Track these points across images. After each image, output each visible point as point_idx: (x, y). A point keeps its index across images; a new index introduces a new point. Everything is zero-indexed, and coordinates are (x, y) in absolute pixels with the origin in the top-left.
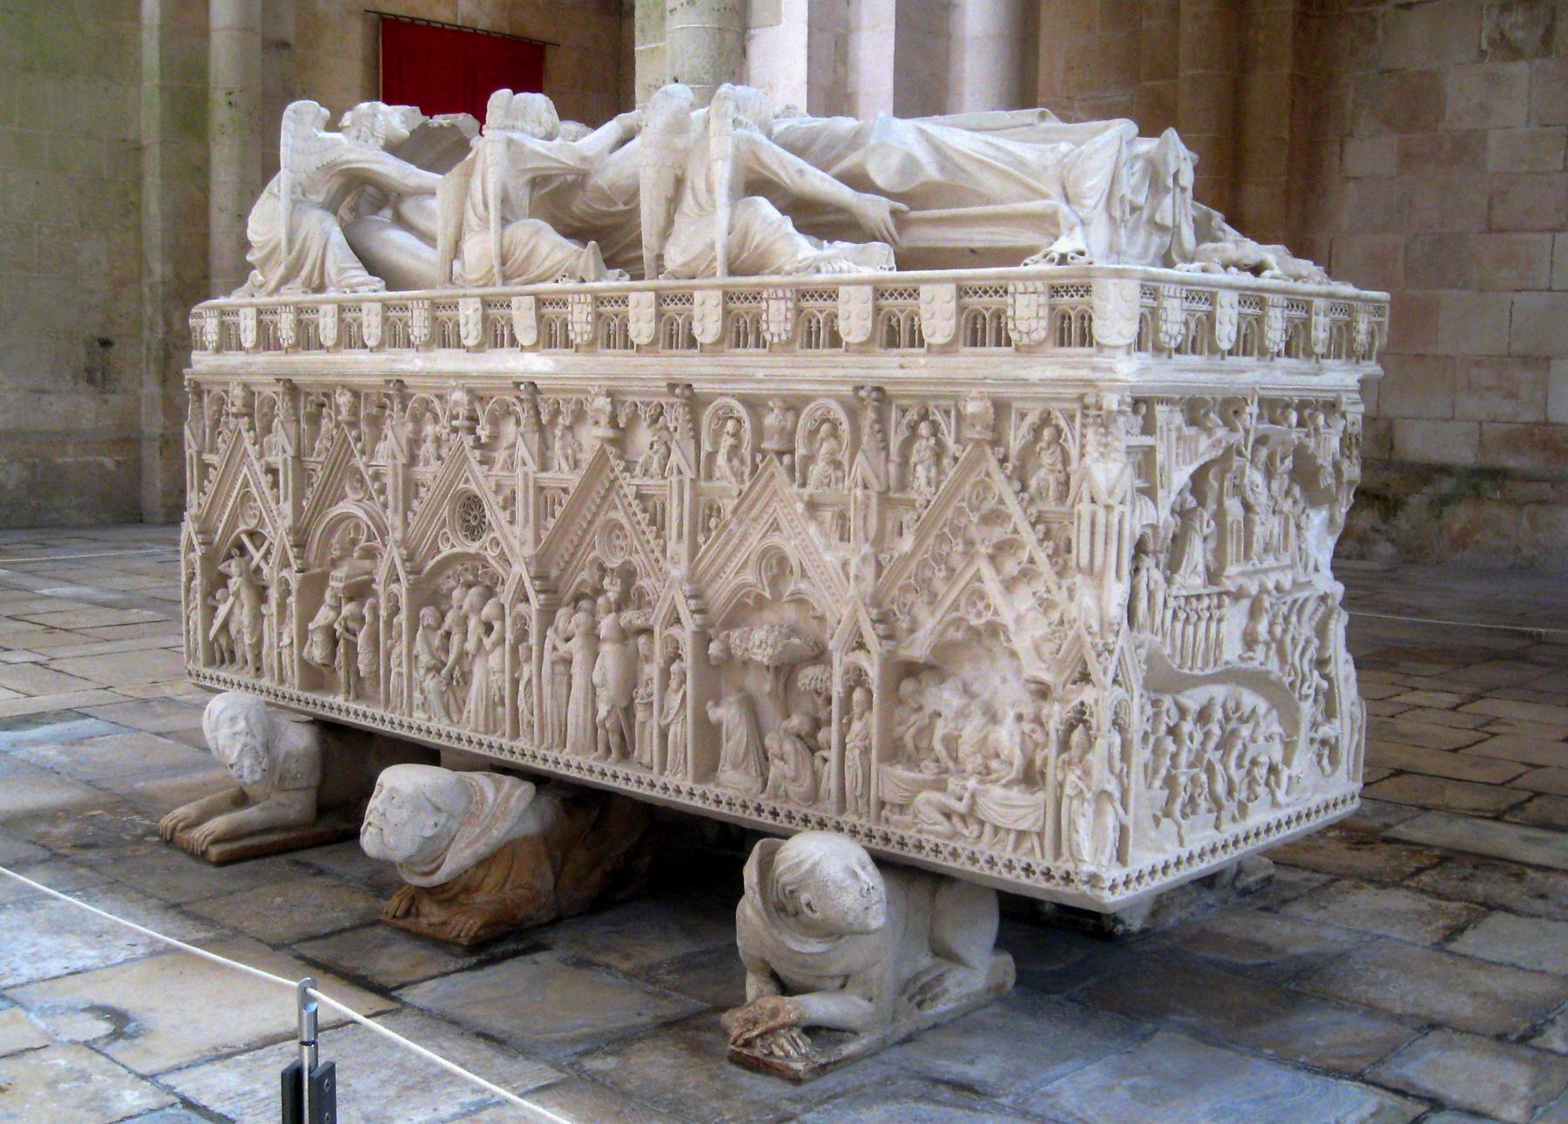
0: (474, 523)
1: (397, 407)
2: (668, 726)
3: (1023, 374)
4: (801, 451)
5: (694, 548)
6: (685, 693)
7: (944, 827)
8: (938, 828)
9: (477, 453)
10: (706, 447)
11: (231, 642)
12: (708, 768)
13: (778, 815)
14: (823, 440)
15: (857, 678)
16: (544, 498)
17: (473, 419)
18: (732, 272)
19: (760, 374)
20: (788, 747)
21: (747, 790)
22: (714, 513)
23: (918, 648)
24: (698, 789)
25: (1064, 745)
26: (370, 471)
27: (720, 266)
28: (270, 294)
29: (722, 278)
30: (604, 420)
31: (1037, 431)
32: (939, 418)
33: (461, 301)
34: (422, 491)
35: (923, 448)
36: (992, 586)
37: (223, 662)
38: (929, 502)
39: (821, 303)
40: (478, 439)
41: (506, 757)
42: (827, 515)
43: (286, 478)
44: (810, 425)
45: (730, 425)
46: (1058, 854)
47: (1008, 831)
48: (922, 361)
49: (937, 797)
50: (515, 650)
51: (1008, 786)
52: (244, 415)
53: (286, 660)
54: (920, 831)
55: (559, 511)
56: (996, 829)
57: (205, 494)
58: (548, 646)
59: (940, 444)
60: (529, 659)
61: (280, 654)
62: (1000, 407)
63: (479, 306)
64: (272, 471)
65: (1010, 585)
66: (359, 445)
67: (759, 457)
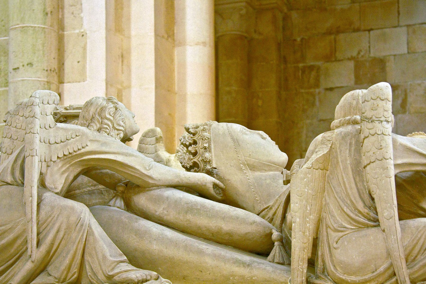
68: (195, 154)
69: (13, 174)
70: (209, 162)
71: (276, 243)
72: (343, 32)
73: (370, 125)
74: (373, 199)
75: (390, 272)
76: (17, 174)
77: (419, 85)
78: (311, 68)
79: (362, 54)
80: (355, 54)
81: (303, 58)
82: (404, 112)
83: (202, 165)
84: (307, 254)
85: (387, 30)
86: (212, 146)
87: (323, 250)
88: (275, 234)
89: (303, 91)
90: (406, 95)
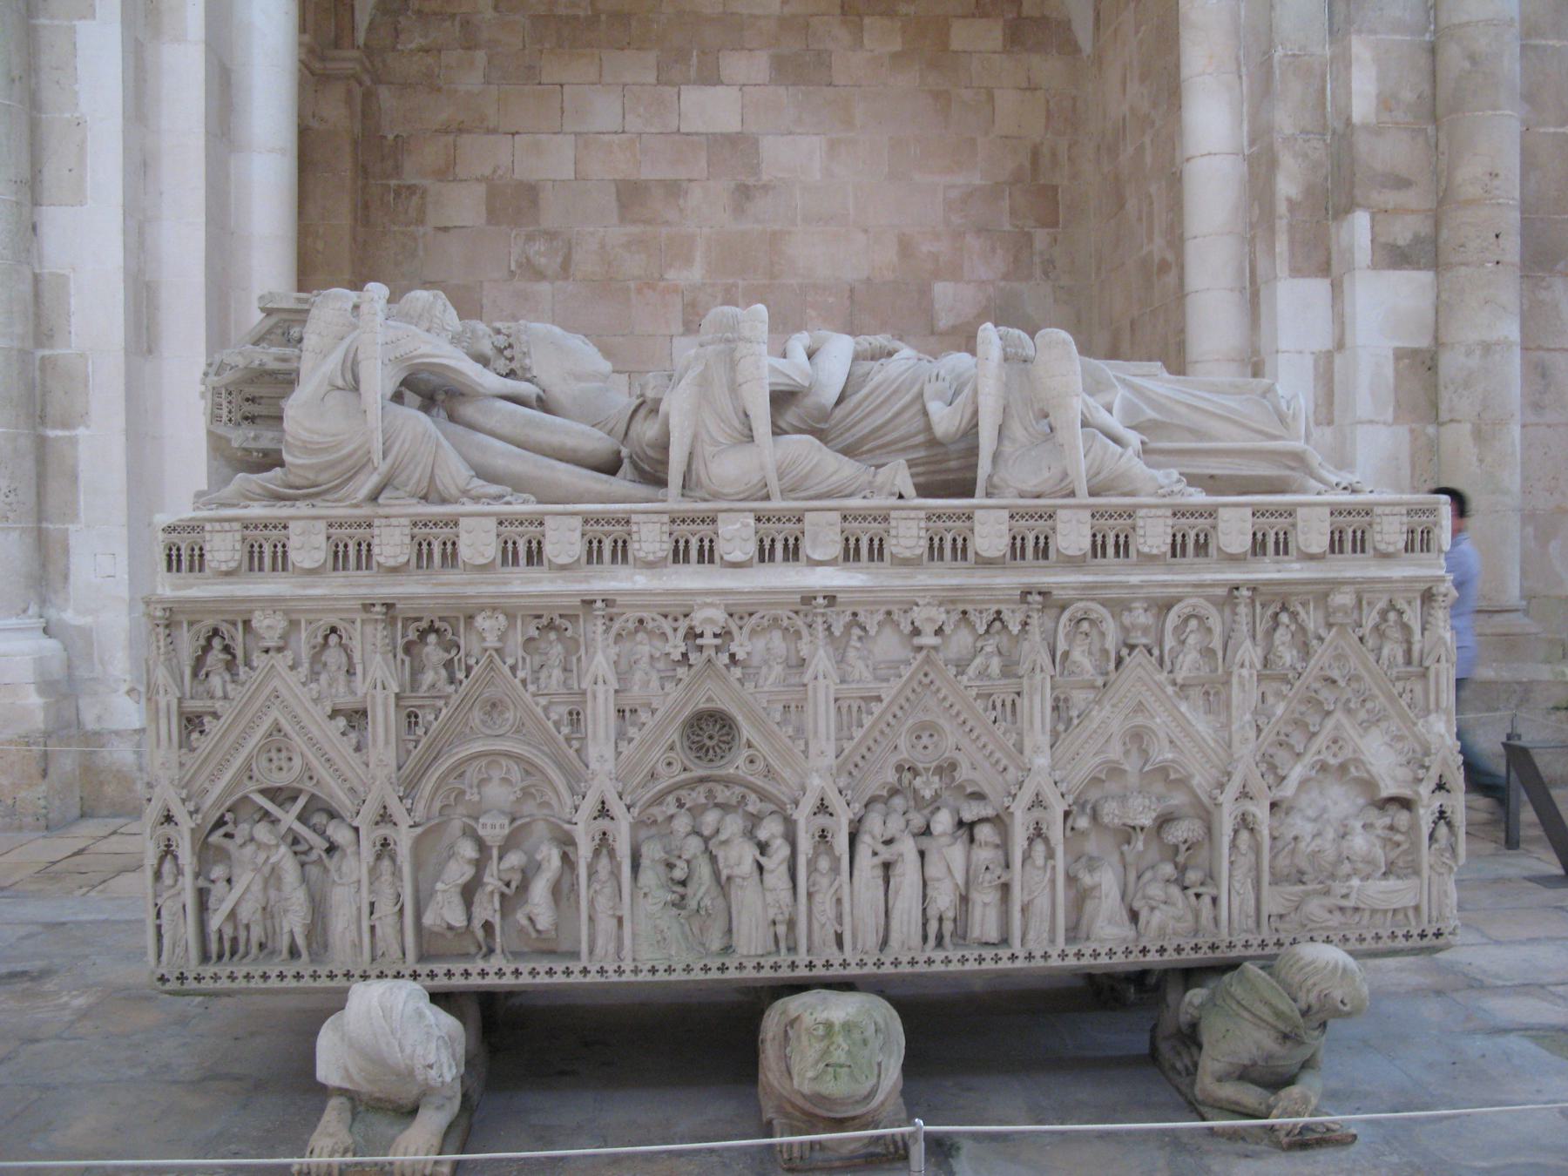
0: (709, 743)
1: (600, 629)
2: (1030, 902)
3: (1385, 574)
4: (1169, 642)
5: (1055, 735)
6: (1054, 868)
7: (1336, 919)
8: (1330, 923)
9: (737, 672)
10: (1062, 646)
11: (236, 928)
12: (1073, 933)
13: (1165, 950)
14: (1192, 631)
15: (1245, 823)
16: (850, 710)
17: (725, 634)
18: (1091, 494)
19: (1134, 579)
20: (1175, 891)
21: (1125, 940)
22: (1061, 704)
23: (1288, 790)
24: (1071, 950)
25: (1432, 837)
26: (543, 701)
27: (1082, 488)
28: (356, 506)
29: (1083, 498)
30: (929, 629)
31: (1383, 615)
32: (1300, 609)
33: (721, 516)
34: (644, 716)
35: (1281, 636)
36: (1350, 731)
37: (220, 957)
38: (1300, 674)
39: (1192, 520)
40: (732, 656)
41: (802, 972)
42: (1195, 693)
43: (384, 720)
44: (1177, 621)
45: (1085, 626)
46: (1429, 922)
47: (1385, 911)
48: (1297, 566)
49: (1329, 901)
50: (812, 865)
51: (1379, 879)
52: (280, 650)
53: (386, 929)
54: (1310, 930)
55: (868, 721)
56: (1374, 912)
57: (193, 750)
58: (864, 851)
59: (1302, 629)
60: (835, 870)
61: (373, 928)
62: (1360, 601)
63: (752, 522)
64: (356, 717)
65: (1366, 729)
66: (521, 674)
67: (1125, 652)
68: (511, 359)
69: (344, 379)
70: (529, 369)
71: (626, 462)
72: (469, 131)
73: (748, 345)
74: (746, 415)
75: (762, 483)
76: (349, 377)
77: (592, 234)
78: (412, 189)
79: (500, 172)
80: (488, 172)
81: (397, 170)
82: (566, 278)
83: (519, 372)
84: (683, 467)
85: (544, 137)
86: (532, 350)
87: (698, 465)
88: (625, 452)
89: (396, 228)
90: (570, 249)
